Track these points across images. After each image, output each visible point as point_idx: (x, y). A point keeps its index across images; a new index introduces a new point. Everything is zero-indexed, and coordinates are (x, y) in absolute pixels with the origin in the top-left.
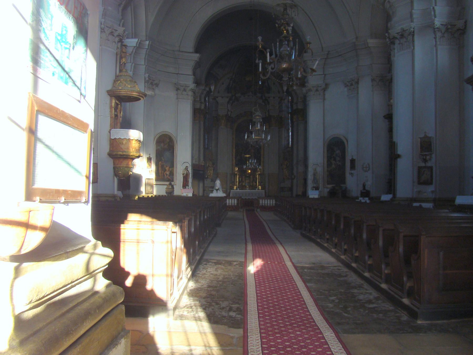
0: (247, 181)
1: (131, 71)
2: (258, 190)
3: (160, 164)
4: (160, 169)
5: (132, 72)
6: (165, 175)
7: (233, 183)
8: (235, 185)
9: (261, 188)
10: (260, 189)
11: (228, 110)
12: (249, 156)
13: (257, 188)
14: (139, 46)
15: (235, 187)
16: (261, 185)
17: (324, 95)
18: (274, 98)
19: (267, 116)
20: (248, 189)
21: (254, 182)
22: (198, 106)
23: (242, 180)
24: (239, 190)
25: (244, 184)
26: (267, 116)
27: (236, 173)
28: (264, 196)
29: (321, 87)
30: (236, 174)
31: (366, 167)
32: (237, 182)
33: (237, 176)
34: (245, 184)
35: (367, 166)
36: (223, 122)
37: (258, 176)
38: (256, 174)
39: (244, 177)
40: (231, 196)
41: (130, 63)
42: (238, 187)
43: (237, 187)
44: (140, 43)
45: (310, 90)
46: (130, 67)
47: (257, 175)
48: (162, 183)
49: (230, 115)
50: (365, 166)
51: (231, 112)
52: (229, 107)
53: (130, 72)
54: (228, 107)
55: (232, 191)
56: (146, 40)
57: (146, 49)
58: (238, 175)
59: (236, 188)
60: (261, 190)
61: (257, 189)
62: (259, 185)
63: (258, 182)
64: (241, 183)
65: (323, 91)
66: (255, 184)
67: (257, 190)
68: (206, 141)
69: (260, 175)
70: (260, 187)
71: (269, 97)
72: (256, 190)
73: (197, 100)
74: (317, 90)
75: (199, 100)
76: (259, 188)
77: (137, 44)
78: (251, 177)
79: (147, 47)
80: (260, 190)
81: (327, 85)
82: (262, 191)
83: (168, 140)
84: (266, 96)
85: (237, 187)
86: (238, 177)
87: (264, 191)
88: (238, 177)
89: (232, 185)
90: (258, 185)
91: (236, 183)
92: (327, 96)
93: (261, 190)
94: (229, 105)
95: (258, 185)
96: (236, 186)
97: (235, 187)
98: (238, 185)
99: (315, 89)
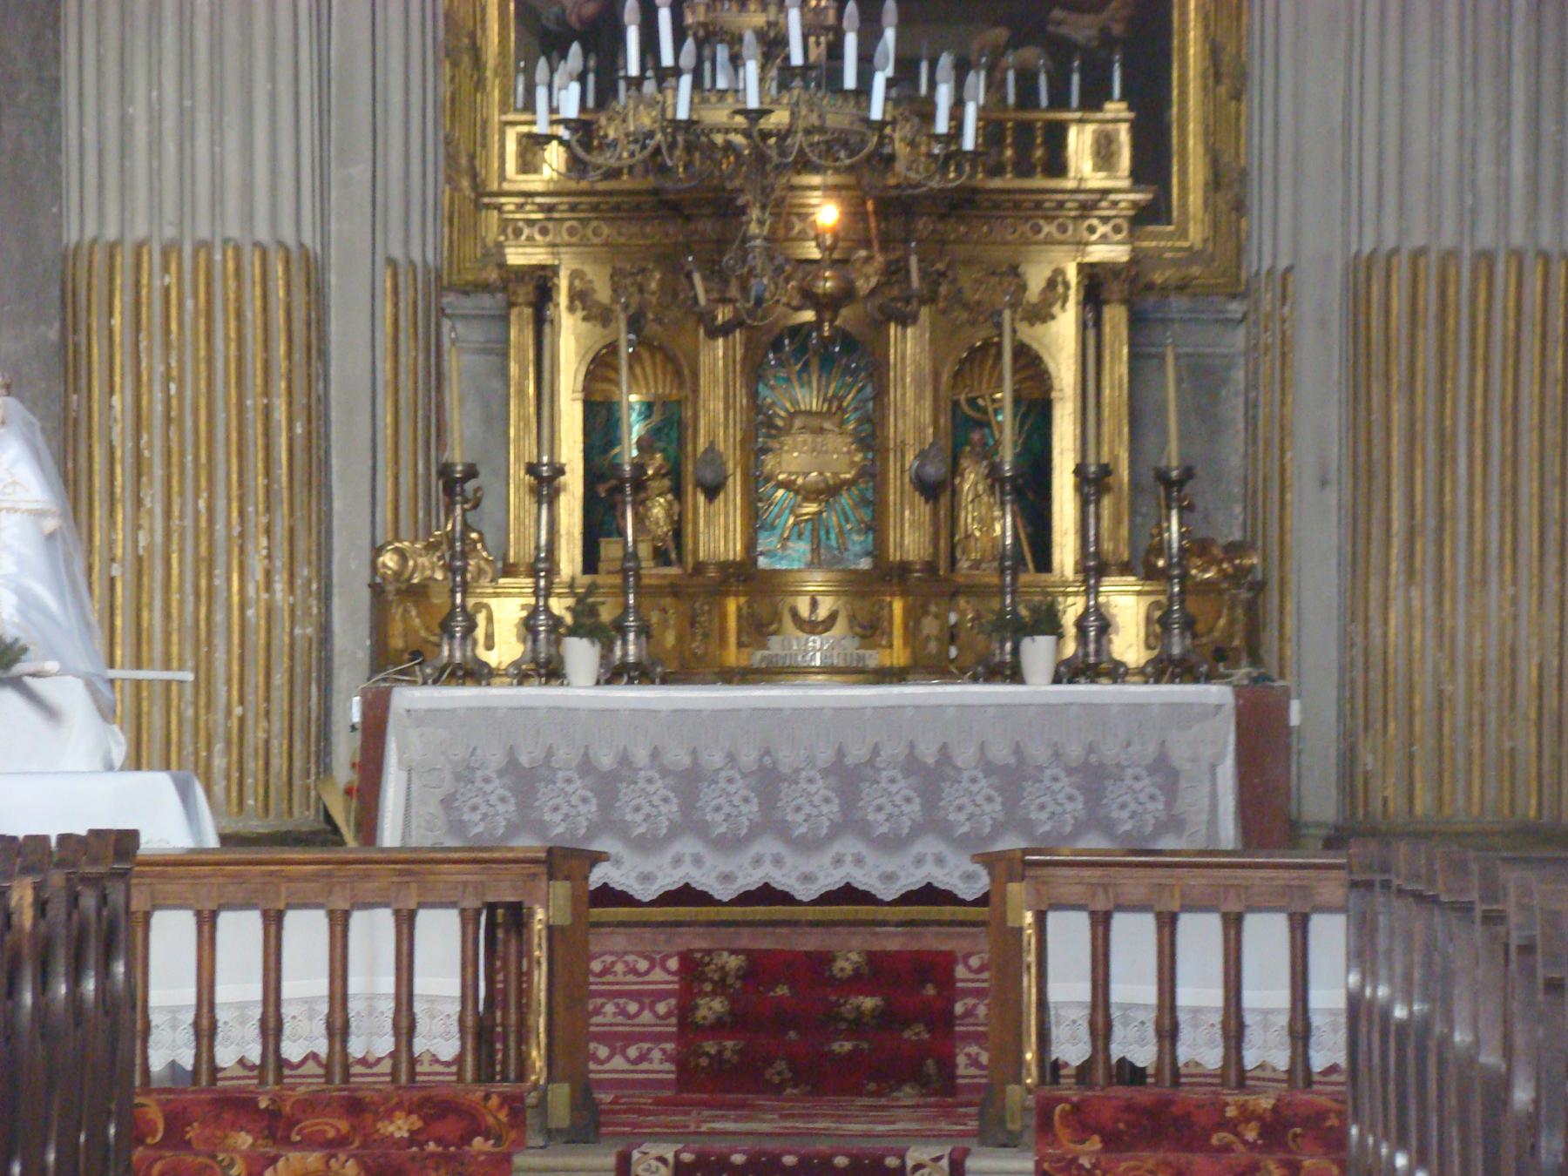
2: (1068, 672)
9: (1159, 625)
10: (1129, 645)
13: (1048, 623)
20: (816, 649)
21: (971, 480)
24: (614, 674)
27: (516, 257)
28: (1228, 834)
30: (541, 284)
32: (545, 484)
34: (755, 521)
37: (1091, 324)
38: (1036, 279)
39: (716, 356)
40: (390, 834)
42: (586, 624)
43: (559, 606)
47: (1041, 314)
55: (409, 698)
58: (580, 297)
59: (528, 626)
60: (1162, 669)
61: (1038, 653)
62: (1094, 568)
63: (1092, 483)
64: (658, 509)
66: (1004, 527)
67: (1038, 686)
69: (1115, 317)
72: (1014, 674)
76: (1098, 624)
80: (1117, 672)
85: (559, 606)
87: (1217, 694)
89: (427, 567)
93: (1162, 669)
96: (543, 567)
98: (570, 560)
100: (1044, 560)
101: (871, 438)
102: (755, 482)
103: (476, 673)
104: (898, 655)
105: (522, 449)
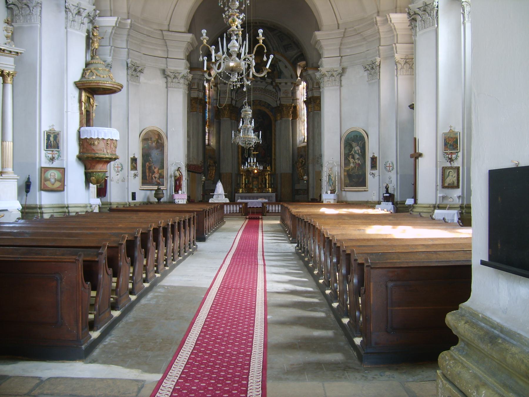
0: (254, 183)
1: (110, 56)
3: (148, 166)
4: (147, 170)
5: (111, 57)
6: (154, 178)
7: (238, 186)
8: (240, 188)
11: (232, 99)
12: (257, 153)
14: (119, 26)
15: (241, 190)
16: (271, 188)
17: (341, 81)
18: (286, 83)
19: (278, 105)
20: (255, 192)
22: (195, 94)
23: (248, 181)
25: (251, 186)
26: (278, 105)
27: (241, 173)
29: (337, 71)
30: (242, 174)
31: (389, 167)
32: (243, 184)
33: (242, 176)
34: (253, 186)
35: (391, 165)
36: (227, 113)
37: (268, 176)
41: (110, 46)
44: (120, 22)
45: (324, 75)
46: (109, 51)
48: (147, 187)
49: (234, 105)
50: (388, 165)
51: (236, 101)
52: (233, 95)
53: (109, 57)
54: (231, 95)
56: (128, 19)
57: (128, 30)
60: (272, 192)
62: (269, 188)
65: (339, 76)
68: (207, 137)
69: (270, 176)
70: (270, 189)
71: (280, 83)
73: (193, 87)
74: (332, 75)
75: (196, 87)
77: (116, 24)
78: (260, 177)
79: (129, 27)
80: (270, 193)
81: (344, 70)
82: (272, 194)
83: (157, 137)
84: (276, 82)
86: (244, 177)
88: (244, 177)
90: (267, 187)
91: (241, 185)
92: (343, 83)
93: (272, 192)
94: (233, 93)
95: (267, 187)
97: (241, 190)
99: (330, 73)
100: (266, 187)
101: (258, 182)
102: (253, 184)
103: (240, 193)
104: (259, 192)
105: (241, 182)
